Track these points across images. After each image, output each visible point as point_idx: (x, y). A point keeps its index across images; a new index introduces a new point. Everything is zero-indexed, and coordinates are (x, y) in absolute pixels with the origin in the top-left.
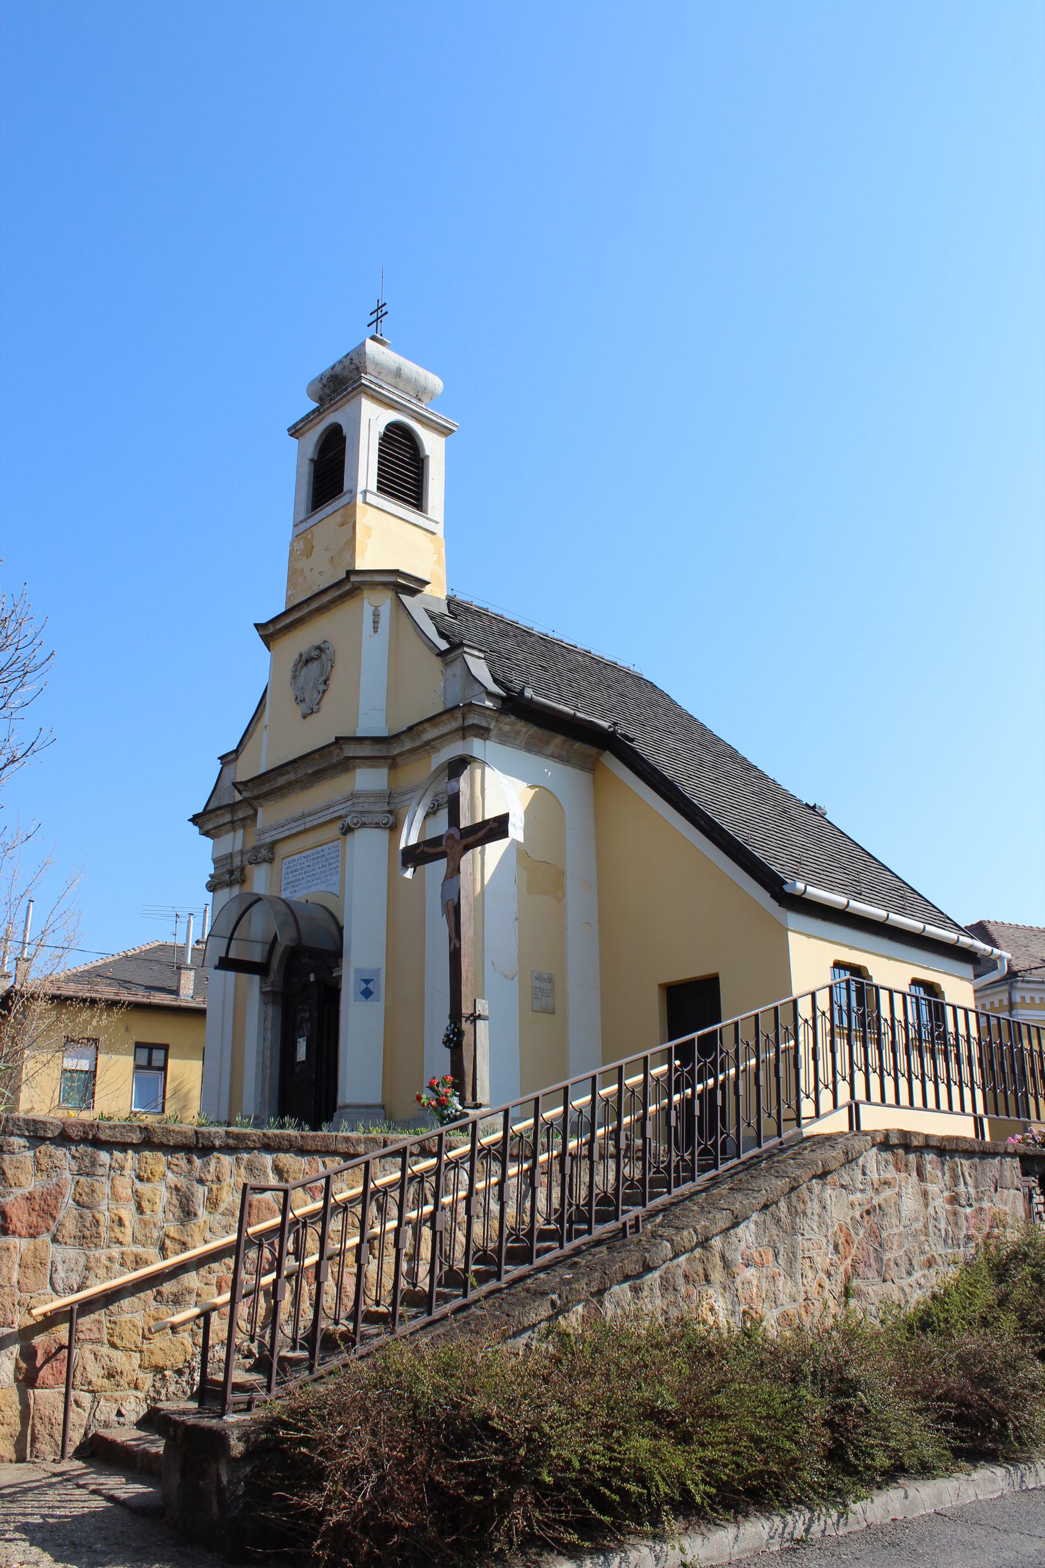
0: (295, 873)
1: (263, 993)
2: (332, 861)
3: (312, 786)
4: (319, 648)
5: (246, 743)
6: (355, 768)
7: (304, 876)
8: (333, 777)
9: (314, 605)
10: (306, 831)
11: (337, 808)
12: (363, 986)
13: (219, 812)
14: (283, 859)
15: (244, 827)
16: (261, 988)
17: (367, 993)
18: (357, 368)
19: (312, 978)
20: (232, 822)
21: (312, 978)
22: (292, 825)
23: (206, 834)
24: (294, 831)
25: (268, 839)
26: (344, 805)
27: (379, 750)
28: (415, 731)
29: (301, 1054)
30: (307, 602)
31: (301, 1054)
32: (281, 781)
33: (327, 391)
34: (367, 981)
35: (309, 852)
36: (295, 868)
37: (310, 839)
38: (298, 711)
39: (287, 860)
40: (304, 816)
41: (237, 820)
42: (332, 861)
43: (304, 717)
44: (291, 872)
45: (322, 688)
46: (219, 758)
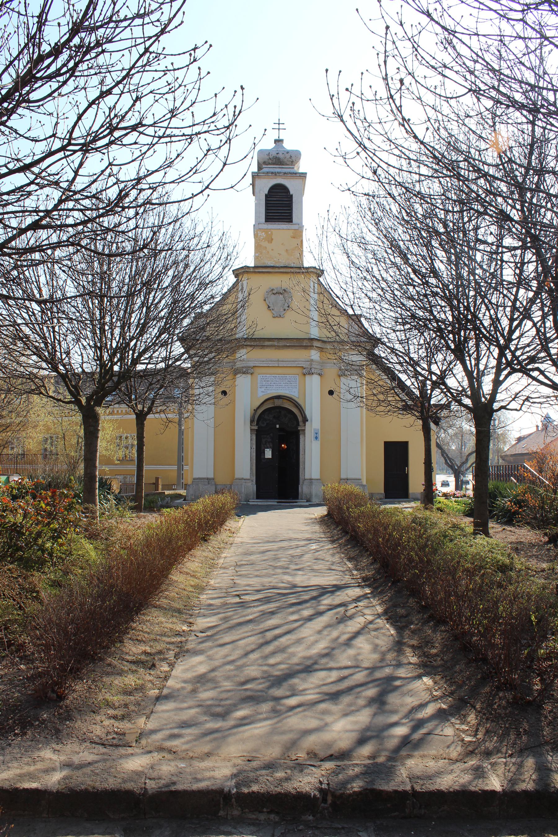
4: (284, 290)
9: (282, 270)
17: (316, 438)
18: (292, 162)
19: (278, 426)
21: (278, 426)
25: (251, 364)
29: (268, 454)
30: (282, 267)
31: (268, 454)
32: (267, 343)
33: (270, 162)
37: (279, 371)
38: (269, 314)
45: (287, 308)
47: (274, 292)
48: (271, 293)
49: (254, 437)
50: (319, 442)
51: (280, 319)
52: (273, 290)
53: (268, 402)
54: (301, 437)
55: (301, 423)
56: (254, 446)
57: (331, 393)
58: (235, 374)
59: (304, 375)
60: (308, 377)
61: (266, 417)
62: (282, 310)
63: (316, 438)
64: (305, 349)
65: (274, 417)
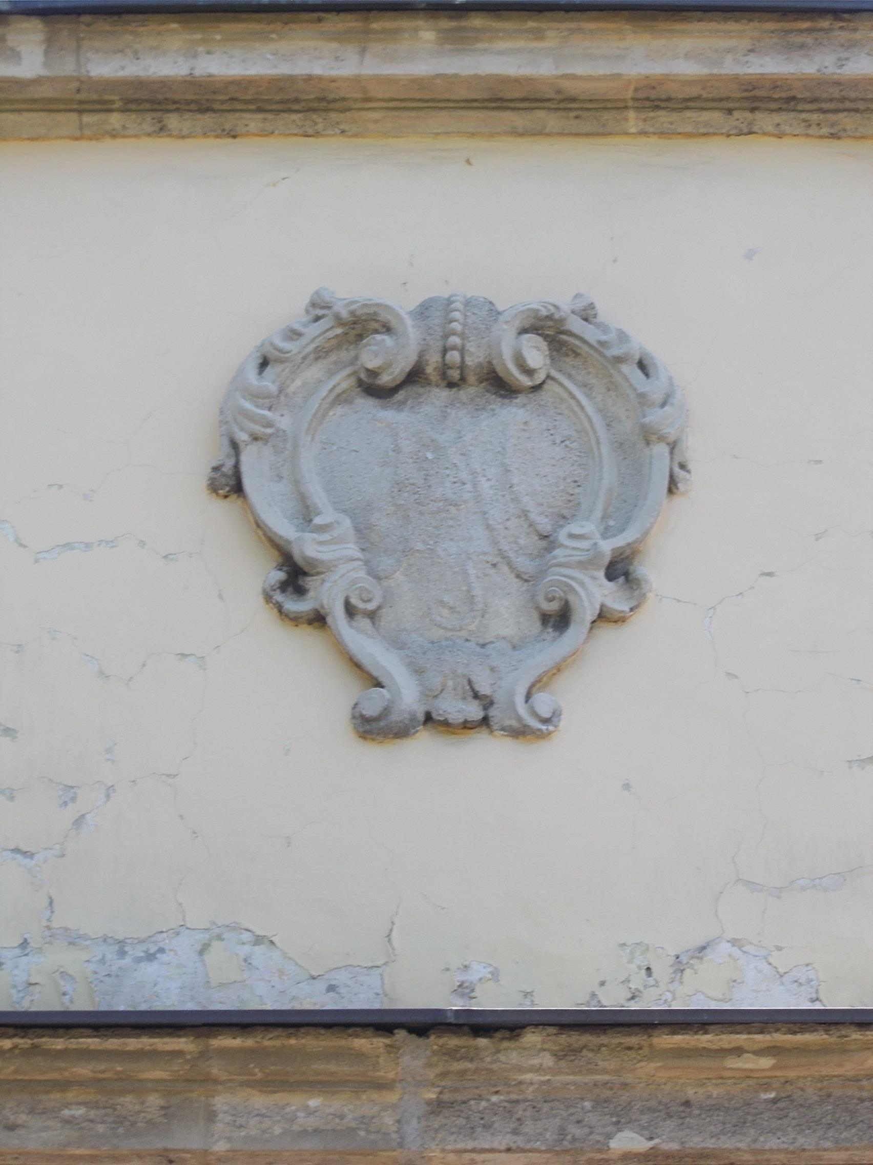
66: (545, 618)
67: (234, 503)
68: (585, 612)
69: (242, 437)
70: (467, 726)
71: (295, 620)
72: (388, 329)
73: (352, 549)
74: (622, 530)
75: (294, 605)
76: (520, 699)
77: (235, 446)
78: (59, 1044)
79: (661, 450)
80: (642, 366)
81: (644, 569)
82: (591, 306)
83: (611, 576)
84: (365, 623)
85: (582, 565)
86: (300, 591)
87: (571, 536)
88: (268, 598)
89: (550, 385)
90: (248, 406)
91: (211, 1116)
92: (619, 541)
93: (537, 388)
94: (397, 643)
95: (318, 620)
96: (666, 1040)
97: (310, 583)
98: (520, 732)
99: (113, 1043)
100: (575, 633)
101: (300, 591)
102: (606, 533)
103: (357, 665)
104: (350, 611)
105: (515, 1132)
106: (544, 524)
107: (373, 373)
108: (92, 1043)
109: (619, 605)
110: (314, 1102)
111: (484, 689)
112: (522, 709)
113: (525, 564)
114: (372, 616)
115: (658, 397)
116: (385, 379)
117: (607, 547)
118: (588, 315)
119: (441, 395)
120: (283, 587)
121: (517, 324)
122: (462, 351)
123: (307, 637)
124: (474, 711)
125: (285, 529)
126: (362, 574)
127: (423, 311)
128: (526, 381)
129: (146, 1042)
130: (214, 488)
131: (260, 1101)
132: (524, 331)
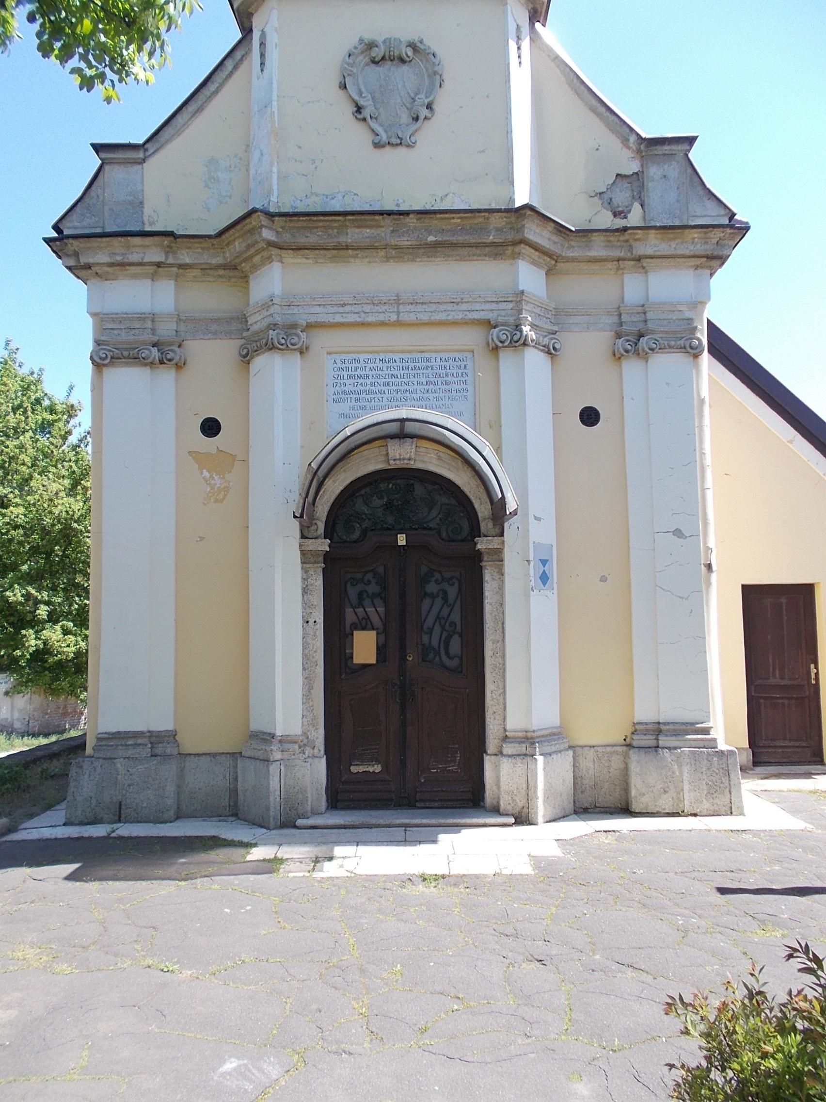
0: (360, 381)
1: (304, 554)
2: (450, 379)
3: (413, 260)
4: (412, 46)
5: (168, 142)
6: (515, 256)
7: (386, 389)
8: (462, 259)
10: (399, 324)
11: (477, 307)
12: (542, 569)
13: (137, 241)
14: (329, 353)
15: (177, 277)
16: (300, 546)
17: (544, 578)
20: (159, 265)
21: (402, 540)
22: (367, 308)
23: (79, 270)
24: (371, 319)
26: (494, 306)
27: (555, 243)
28: (626, 236)
32: (354, 235)
34: (544, 562)
35: (396, 357)
36: (359, 372)
39: (329, 357)
40: (398, 301)
41: (171, 265)
42: (450, 379)
43: (377, 145)
44: (350, 377)
45: (424, 112)
46: (98, 148)
47: (377, 53)
48: (363, 59)
49: (318, 582)
50: (553, 595)
51: (401, 150)
52: (371, 46)
53: (367, 452)
54: (487, 575)
55: (486, 526)
56: (318, 615)
57: (590, 416)
58: (246, 357)
59: (495, 350)
60: (506, 358)
61: (360, 506)
62: (405, 118)
63: (544, 578)
64: (496, 256)
65: (389, 506)
66: (413, 119)
67: (345, 91)
68: (422, 117)
69: (346, 75)
70: (397, 145)
71: (359, 119)
72: (377, 46)
73: (371, 102)
74: (430, 97)
75: (359, 116)
76: (408, 141)
77: (344, 77)
78: (315, 218)
79: (438, 77)
80: (433, 55)
81: (434, 107)
82: (422, 40)
83: (427, 108)
84: (375, 120)
85: (421, 106)
86: (360, 113)
87: (419, 99)
88: (353, 115)
89: (413, 60)
90: (347, 66)
91: (347, 234)
92: (430, 99)
93: (411, 61)
94: (381, 125)
95: (364, 119)
96: (438, 216)
97: (362, 110)
98: (408, 146)
99: (326, 218)
100: (420, 121)
101: (360, 113)
102: (426, 97)
103: (373, 130)
104: (371, 117)
105: (409, 237)
106: (413, 95)
107: (374, 58)
108: (322, 218)
109: (429, 115)
110: (368, 231)
111: (400, 136)
112: (408, 141)
113: (409, 106)
114: (376, 119)
115: (437, 63)
116: (377, 59)
117: (426, 101)
118: (421, 42)
119: (389, 63)
120: (356, 112)
121: (406, 45)
122: (394, 51)
123: (362, 123)
124: (398, 141)
125: (356, 98)
126: (373, 108)
127: (384, 42)
128: (408, 59)
129: (333, 218)
130: (340, 87)
131: (357, 230)
132: (407, 46)
